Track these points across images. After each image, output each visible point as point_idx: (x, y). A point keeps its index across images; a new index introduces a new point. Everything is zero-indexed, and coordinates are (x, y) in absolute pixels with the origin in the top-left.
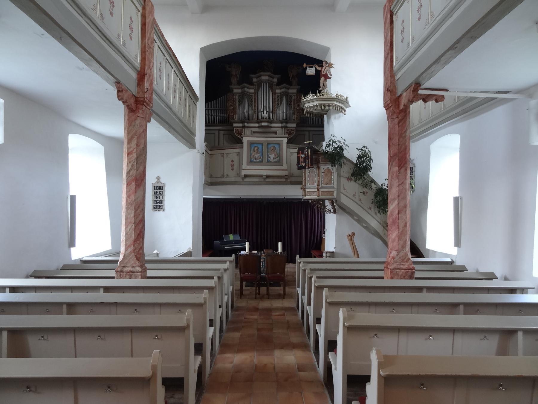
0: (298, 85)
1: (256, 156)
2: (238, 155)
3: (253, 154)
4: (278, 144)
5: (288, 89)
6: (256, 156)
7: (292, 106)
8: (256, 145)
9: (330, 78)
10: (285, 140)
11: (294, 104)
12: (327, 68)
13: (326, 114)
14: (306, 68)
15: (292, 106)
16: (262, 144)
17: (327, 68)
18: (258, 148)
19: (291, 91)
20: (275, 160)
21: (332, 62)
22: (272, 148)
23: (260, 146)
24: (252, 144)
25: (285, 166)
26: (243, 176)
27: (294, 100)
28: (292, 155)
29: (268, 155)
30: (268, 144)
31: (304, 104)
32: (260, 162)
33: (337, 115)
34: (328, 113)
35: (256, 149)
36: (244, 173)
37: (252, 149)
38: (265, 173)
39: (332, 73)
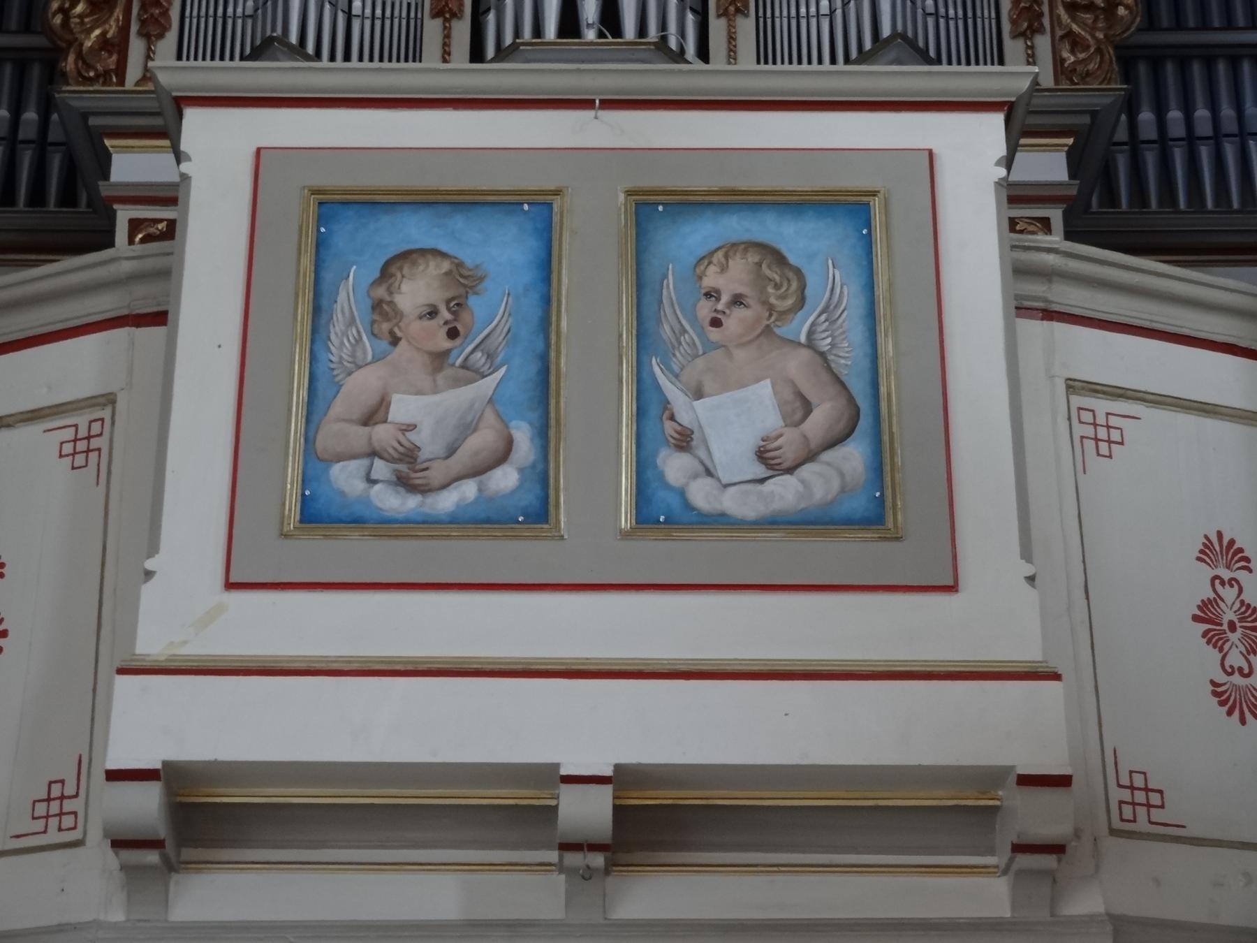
1: (423, 411)
2: (83, 450)
3: (361, 386)
4: (851, 207)
6: (423, 411)
8: (415, 230)
10: (970, 151)
16: (534, 207)
18: (463, 281)
20: (785, 493)
22: (732, 278)
23: (501, 252)
24: (339, 205)
25: (994, 609)
26: (144, 806)
28: (1105, 441)
29: (649, 404)
30: (656, 206)
32: (485, 521)
35: (415, 291)
36: (154, 726)
37: (349, 297)
38: (592, 734)
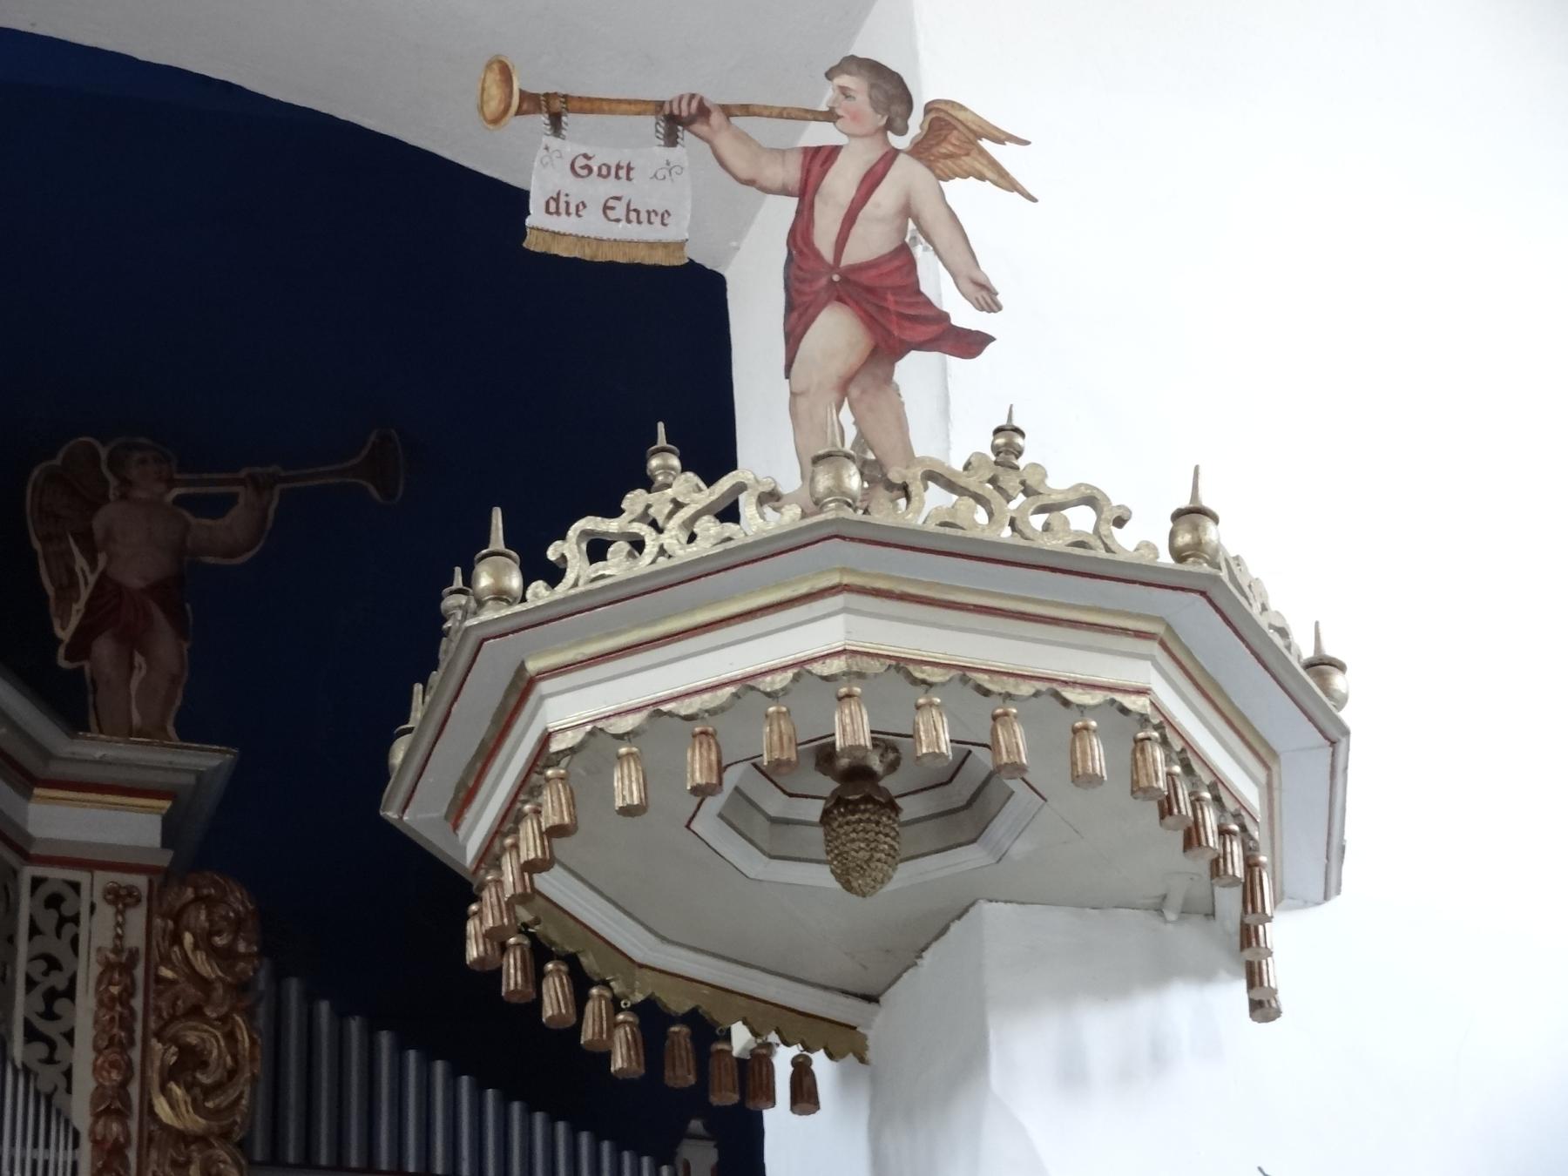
0: (192, 730)
5: (27, 781)
7: (83, 1057)
9: (970, 344)
11: (113, 1044)
12: (907, 175)
13: (844, 1041)
15: (83, 1057)
17: (907, 175)
19: (55, 820)
21: (983, 104)
27: (119, 965)
31: (522, 688)
33: (1103, 1028)
34: (878, 1026)
39: (991, 268)
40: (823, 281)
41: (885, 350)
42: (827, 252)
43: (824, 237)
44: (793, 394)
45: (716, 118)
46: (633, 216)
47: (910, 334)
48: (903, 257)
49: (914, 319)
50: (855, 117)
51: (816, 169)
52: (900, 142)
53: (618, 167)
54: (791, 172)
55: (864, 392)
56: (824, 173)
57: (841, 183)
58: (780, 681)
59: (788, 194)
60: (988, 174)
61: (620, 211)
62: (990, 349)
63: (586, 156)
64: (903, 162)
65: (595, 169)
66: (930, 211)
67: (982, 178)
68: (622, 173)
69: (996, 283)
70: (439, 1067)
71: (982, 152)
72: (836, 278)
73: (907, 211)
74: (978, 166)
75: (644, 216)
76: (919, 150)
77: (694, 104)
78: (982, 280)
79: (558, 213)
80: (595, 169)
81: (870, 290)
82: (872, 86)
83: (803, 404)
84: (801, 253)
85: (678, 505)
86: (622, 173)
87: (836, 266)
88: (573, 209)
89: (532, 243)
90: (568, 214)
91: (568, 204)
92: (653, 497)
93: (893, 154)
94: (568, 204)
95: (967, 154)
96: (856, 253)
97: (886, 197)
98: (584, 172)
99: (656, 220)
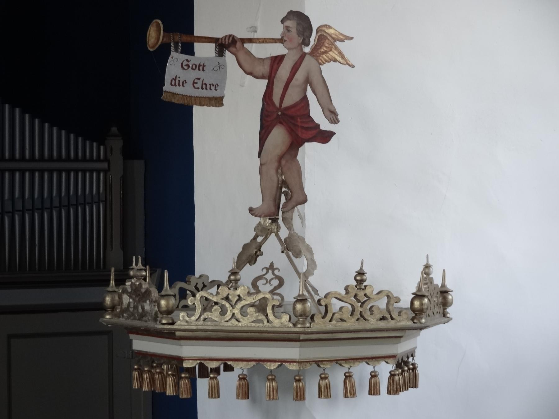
9: (325, 137)
14: (163, 53)
40: (275, 116)
41: (295, 144)
42: (277, 103)
43: (276, 99)
44: (261, 165)
45: (238, 44)
46: (204, 86)
47: (304, 136)
48: (305, 100)
49: (307, 129)
50: (291, 40)
51: (275, 67)
52: (307, 50)
53: (200, 65)
54: (265, 69)
55: (287, 162)
56: (279, 67)
57: (284, 71)
58: (273, 366)
59: (263, 77)
60: (338, 58)
61: (199, 85)
62: (334, 139)
63: (187, 61)
64: (307, 58)
65: (191, 66)
66: (315, 79)
67: (335, 61)
68: (201, 68)
69: (338, 111)
70: (17, 110)
71: (336, 48)
72: (279, 113)
73: (308, 81)
74: (334, 55)
75: (208, 87)
76: (315, 52)
77: (231, 39)
78: (332, 110)
79: (175, 85)
80: (191, 66)
81: (292, 118)
82: (298, 24)
83: (264, 168)
84: (267, 103)
85: (240, 298)
86: (201, 68)
87: (280, 109)
88: (181, 84)
89: (164, 97)
90: (179, 85)
91: (179, 81)
92: (231, 292)
93: (304, 55)
94: (179, 81)
95: (331, 50)
96: (289, 101)
97: (300, 76)
98: (186, 68)
99: (213, 88)
